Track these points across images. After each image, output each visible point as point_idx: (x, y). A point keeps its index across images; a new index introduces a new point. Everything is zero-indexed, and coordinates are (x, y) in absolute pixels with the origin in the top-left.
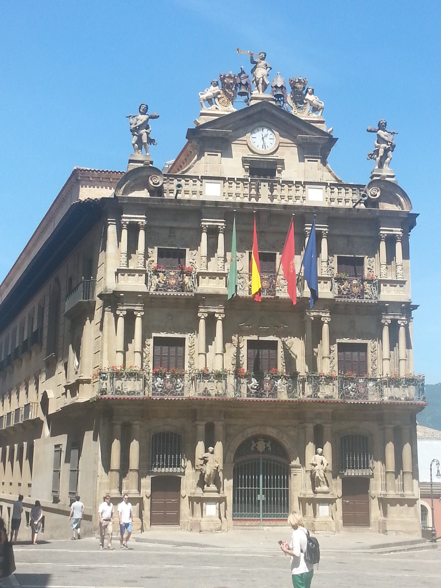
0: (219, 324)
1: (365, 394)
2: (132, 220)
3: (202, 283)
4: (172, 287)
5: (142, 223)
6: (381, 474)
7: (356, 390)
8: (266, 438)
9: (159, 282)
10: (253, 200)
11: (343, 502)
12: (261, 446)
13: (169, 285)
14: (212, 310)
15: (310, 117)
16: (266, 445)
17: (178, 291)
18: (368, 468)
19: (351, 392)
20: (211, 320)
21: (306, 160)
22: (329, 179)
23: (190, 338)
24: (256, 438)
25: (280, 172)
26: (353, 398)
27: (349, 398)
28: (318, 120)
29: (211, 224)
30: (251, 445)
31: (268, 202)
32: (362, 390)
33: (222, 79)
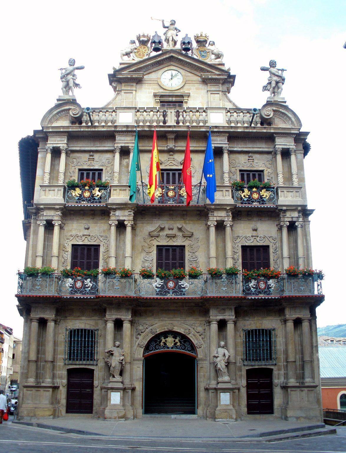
0: (129, 229)
1: (265, 290)
2: (55, 145)
3: (114, 195)
4: (87, 200)
5: (63, 147)
6: (284, 365)
7: (257, 287)
8: (175, 334)
9: (75, 195)
10: (161, 124)
11: (247, 392)
12: (170, 341)
13: (84, 197)
14: (122, 218)
15: (212, 62)
16: (175, 341)
17: (91, 203)
18: (271, 359)
19: (252, 289)
20: (121, 226)
21: (209, 93)
22: (229, 106)
23: (105, 245)
24: (165, 334)
25: (186, 102)
26: (254, 294)
27: (250, 294)
28: (219, 63)
29: (123, 145)
30: (161, 341)
31: (175, 124)
32: (262, 286)
33: (138, 38)
